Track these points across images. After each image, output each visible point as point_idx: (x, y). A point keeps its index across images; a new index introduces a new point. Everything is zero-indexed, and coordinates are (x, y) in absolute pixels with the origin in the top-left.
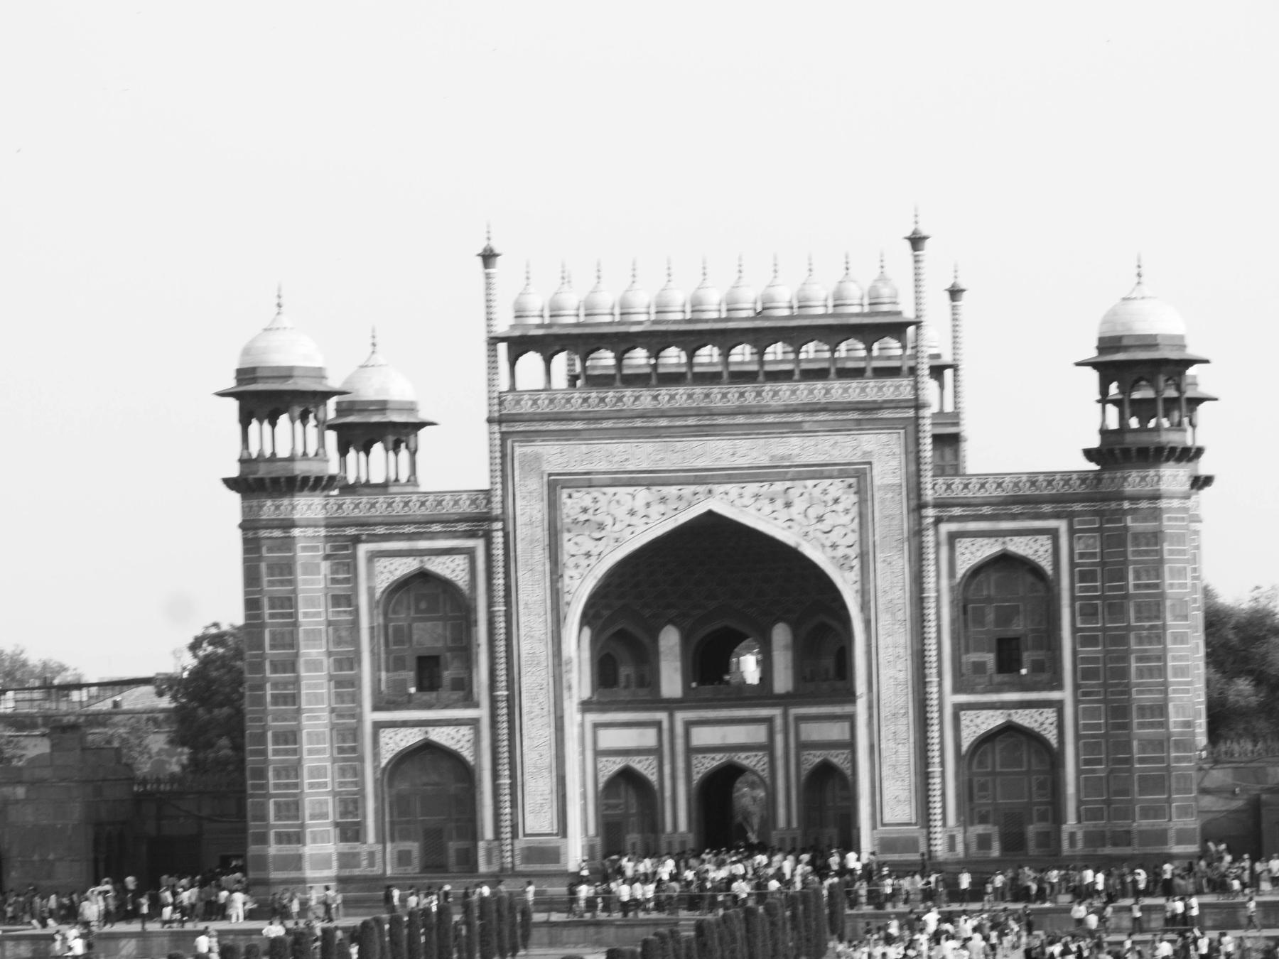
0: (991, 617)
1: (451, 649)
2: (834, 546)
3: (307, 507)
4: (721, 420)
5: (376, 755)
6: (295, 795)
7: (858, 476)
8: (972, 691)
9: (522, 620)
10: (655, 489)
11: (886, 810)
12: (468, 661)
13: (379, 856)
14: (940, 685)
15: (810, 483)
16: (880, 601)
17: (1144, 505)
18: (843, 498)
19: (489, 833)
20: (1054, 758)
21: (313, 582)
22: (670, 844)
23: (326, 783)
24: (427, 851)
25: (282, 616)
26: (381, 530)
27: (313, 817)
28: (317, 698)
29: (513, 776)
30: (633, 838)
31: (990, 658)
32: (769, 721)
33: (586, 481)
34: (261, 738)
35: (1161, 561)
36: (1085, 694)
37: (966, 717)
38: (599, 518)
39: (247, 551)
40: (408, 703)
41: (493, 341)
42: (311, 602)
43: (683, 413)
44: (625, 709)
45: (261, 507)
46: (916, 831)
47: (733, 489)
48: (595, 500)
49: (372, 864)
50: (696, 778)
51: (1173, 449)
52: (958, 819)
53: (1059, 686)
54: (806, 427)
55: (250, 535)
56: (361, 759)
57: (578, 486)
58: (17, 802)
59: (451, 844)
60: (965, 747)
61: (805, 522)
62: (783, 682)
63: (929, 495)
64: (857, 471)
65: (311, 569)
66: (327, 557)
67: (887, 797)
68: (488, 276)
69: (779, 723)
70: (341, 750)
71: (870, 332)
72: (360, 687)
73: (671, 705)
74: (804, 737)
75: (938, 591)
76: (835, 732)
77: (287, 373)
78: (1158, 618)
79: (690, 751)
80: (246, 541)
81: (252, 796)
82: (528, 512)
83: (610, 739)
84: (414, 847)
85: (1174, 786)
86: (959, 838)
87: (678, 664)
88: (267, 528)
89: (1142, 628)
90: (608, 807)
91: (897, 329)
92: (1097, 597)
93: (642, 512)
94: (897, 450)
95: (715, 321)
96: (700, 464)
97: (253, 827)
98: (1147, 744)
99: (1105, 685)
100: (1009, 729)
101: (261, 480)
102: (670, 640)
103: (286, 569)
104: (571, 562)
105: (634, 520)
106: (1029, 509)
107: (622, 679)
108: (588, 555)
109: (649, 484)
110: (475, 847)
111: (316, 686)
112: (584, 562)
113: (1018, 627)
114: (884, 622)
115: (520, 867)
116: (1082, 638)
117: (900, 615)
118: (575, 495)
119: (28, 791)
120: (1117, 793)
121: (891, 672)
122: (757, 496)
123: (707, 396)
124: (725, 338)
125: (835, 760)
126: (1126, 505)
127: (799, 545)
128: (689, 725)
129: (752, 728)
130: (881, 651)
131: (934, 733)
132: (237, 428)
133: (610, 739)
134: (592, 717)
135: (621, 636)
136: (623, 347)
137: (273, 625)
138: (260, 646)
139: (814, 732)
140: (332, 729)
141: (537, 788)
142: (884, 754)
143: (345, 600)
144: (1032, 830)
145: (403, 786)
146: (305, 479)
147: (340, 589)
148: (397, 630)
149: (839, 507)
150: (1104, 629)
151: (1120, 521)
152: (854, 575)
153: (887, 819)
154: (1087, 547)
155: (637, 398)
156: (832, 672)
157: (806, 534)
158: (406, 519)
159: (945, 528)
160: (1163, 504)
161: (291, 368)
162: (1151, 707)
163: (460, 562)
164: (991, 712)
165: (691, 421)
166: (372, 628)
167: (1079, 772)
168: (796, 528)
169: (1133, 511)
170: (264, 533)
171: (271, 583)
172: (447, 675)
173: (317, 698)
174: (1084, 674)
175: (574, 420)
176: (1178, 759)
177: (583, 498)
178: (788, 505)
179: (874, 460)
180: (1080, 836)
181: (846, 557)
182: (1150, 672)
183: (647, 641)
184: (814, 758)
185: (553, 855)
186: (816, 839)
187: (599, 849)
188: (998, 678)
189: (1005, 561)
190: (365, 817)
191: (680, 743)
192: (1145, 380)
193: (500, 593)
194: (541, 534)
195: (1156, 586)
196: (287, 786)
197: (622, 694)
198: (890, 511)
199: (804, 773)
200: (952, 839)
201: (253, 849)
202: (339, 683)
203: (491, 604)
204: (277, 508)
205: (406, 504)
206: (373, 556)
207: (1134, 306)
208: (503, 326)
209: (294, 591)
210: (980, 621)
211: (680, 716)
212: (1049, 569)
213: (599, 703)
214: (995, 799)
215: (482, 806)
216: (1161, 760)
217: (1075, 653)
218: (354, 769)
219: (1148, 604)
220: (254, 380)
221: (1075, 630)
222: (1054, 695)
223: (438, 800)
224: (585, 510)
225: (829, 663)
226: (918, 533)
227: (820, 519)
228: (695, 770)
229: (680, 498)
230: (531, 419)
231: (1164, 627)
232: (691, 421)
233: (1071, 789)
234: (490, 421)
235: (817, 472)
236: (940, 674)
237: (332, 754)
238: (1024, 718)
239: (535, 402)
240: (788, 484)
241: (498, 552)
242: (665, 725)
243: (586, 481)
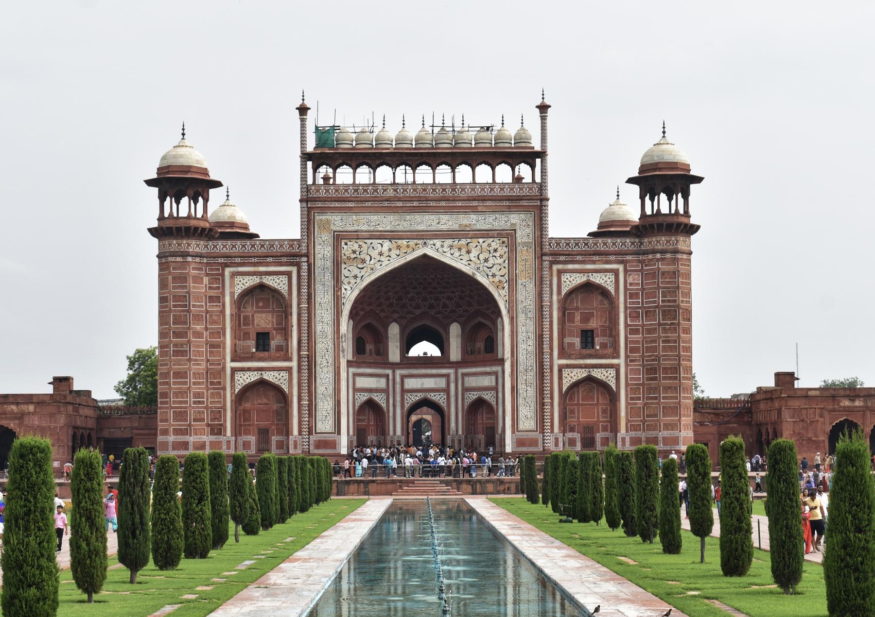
0: (578, 318)
1: (275, 329)
2: (494, 276)
4: (432, 204)
5: (233, 387)
6: (186, 408)
7: (508, 236)
8: (569, 357)
9: (318, 312)
10: (393, 241)
11: (521, 423)
12: (287, 335)
13: (233, 443)
14: (551, 354)
15: (481, 240)
16: (520, 306)
17: (668, 256)
18: (499, 249)
19: (295, 432)
20: (612, 396)
21: (200, 288)
22: (392, 442)
23: (203, 402)
24: (259, 442)
25: (180, 306)
26: (238, 260)
27: (195, 420)
28: (199, 353)
29: (310, 400)
30: (371, 438)
31: (577, 341)
32: (447, 376)
33: (356, 236)
34: (166, 375)
35: (678, 287)
36: (631, 361)
37: (565, 372)
38: (362, 256)
39: (160, 270)
40: (251, 358)
41: (306, 157)
42: (197, 299)
43: (411, 200)
44: (370, 367)
45: (170, 245)
46: (537, 435)
47: (438, 243)
48: (360, 247)
49: (228, 448)
50: (407, 406)
51: (686, 225)
52: (560, 429)
53: (618, 357)
54: (480, 209)
55: (164, 260)
56: (224, 389)
57: (350, 239)
58: (29, 413)
59: (273, 438)
60: (564, 390)
61: (478, 262)
62: (455, 354)
63: (547, 249)
64: (507, 234)
65: (198, 280)
66: (207, 275)
68: (303, 121)
69: (452, 377)
70: (212, 383)
72: (224, 348)
73: (394, 366)
74: (467, 385)
75: (551, 302)
76: (488, 381)
77: (188, 169)
78: (675, 319)
79: (404, 391)
80: (160, 264)
81: (161, 408)
82: (323, 251)
83: (363, 382)
84: (252, 439)
85: (682, 412)
86: (561, 440)
87: (399, 344)
88: (173, 256)
89: (667, 324)
90: (359, 420)
92: (639, 308)
93: (385, 255)
94: (531, 224)
95: (429, 149)
96: (420, 228)
97: (161, 425)
98: (667, 389)
99: (643, 356)
100: (590, 379)
101: (171, 228)
102: (394, 330)
104: (345, 281)
105: (382, 258)
106: (604, 258)
107: (368, 351)
108: (356, 277)
109: (390, 240)
110: (288, 438)
111: (198, 346)
112: (353, 281)
113: (593, 324)
114: (521, 318)
115: (313, 450)
116: (632, 330)
117: (530, 315)
118: (349, 243)
119: (35, 408)
120: (648, 416)
121: (524, 346)
122: (451, 247)
123: (424, 190)
125: (486, 397)
126: (658, 256)
127: (474, 274)
128: (403, 377)
129: (438, 379)
130: (520, 335)
131: (547, 381)
132: (158, 201)
133: (363, 382)
134: (351, 370)
135: (369, 327)
136: (378, 162)
137: (175, 311)
138: (168, 323)
139: (471, 382)
140: (207, 373)
141: (324, 407)
142: (520, 391)
144: (599, 436)
145: (247, 405)
146: (196, 229)
147: (213, 293)
148: (246, 317)
149: (497, 254)
150: (643, 325)
151: (655, 265)
152: (505, 292)
153: (521, 427)
154: (634, 280)
155: (385, 190)
156: (482, 348)
157: (478, 268)
158: (252, 255)
159: (555, 267)
160: (679, 256)
161: (190, 167)
162: (670, 368)
163: (284, 279)
164: (579, 370)
165: (415, 204)
166: (232, 315)
167: (627, 404)
168: (473, 265)
169: (663, 259)
170: (170, 259)
171: (174, 287)
172: (273, 343)
173: (199, 353)
175: (349, 201)
176: (684, 398)
177: (354, 245)
178: (469, 252)
179: (518, 228)
180: (628, 440)
181: (500, 282)
182: (671, 349)
183: (382, 330)
184: (473, 396)
185: (333, 444)
186: (472, 441)
187: (355, 444)
188: (584, 351)
189: (588, 287)
190: (225, 421)
191: (398, 387)
193: (304, 297)
194: (329, 264)
195: (675, 301)
196: (181, 402)
197: (367, 357)
198: (526, 257)
199: (466, 404)
200: (557, 439)
201: (160, 438)
202: (212, 346)
203: (299, 304)
204: (179, 245)
205: (253, 246)
206: (233, 275)
207: (664, 147)
208: (310, 147)
209: (188, 293)
210: (572, 320)
211: (398, 372)
212: (613, 292)
213: (356, 362)
214: (578, 418)
215: (292, 416)
216: (676, 398)
217: (626, 338)
218: (219, 394)
219: (669, 311)
220: (168, 173)
221: (626, 325)
222: (615, 361)
224: (354, 252)
225: (480, 345)
226: (541, 269)
227: (486, 260)
228: (406, 402)
229: (408, 246)
230: (325, 200)
231: (679, 323)
232: (415, 204)
233: (623, 414)
234: (301, 201)
235: (486, 234)
236: (551, 349)
237: (207, 386)
238: (597, 374)
239: (327, 191)
240: (469, 240)
241: (304, 274)
242: (391, 377)
243: (356, 236)
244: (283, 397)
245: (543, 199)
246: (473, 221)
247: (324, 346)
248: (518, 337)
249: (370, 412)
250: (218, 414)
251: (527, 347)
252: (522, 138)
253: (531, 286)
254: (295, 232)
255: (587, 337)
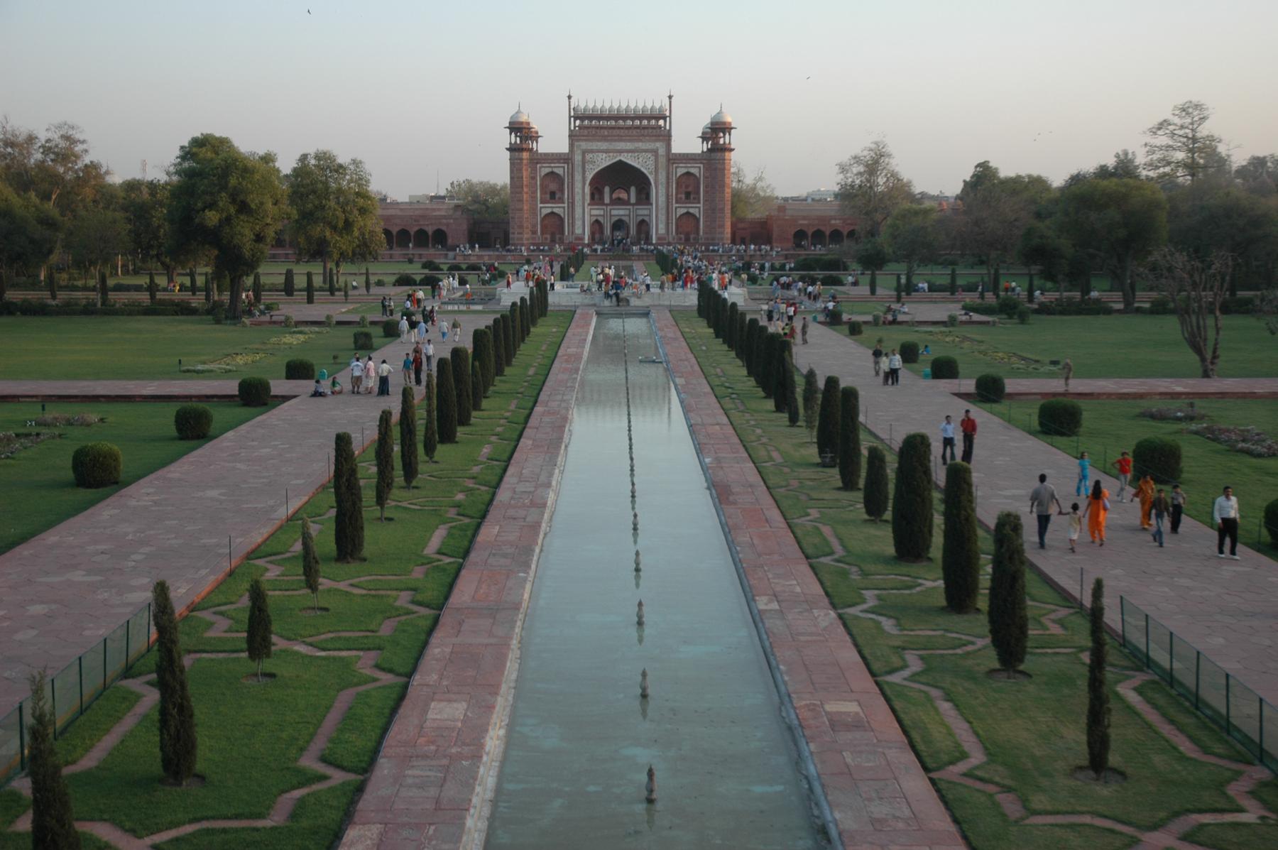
3: (525, 155)
7: (655, 152)
20: (698, 220)
21: (526, 174)
30: (597, 236)
33: (592, 151)
62: (633, 200)
67: (659, 228)
71: (657, 118)
76: (646, 212)
91: (664, 118)
102: (607, 189)
103: (521, 170)
113: (690, 189)
124: (625, 118)
133: (594, 212)
139: (640, 212)
141: (578, 223)
143: (534, 178)
174: (705, 201)
185: (583, 239)
189: (688, 174)
192: (717, 131)
198: (662, 160)
223: (554, 225)
225: (644, 196)
235: (646, 151)
238: (691, 211)
243: (592, 151)
244: (562, 220)
245: (670, 136)
246: (640, 145)
247: (578, 198)
248: (658, 194)
249: (597, 225)
250: (535, 226)
251: (662, 199)
252: (661, 109)
253: (664, 174)
254: (566, 150)
255: (688, 195)
